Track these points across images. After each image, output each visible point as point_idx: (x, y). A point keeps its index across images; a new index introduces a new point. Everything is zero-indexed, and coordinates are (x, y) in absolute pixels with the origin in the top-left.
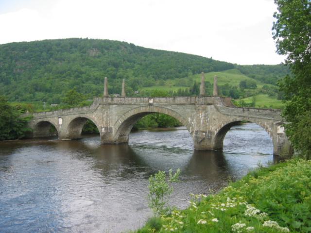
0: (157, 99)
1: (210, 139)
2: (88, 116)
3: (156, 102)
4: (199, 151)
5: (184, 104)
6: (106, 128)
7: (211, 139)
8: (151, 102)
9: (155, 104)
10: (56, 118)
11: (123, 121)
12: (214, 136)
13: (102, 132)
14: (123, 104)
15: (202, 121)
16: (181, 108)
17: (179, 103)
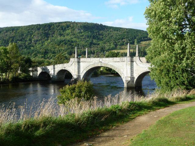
2: (67, 69)
5: (119, 62)
7: (134, 81)
8: (101, 60)
12: (135, 80)
14: (86, 62)
16: (117, 63)
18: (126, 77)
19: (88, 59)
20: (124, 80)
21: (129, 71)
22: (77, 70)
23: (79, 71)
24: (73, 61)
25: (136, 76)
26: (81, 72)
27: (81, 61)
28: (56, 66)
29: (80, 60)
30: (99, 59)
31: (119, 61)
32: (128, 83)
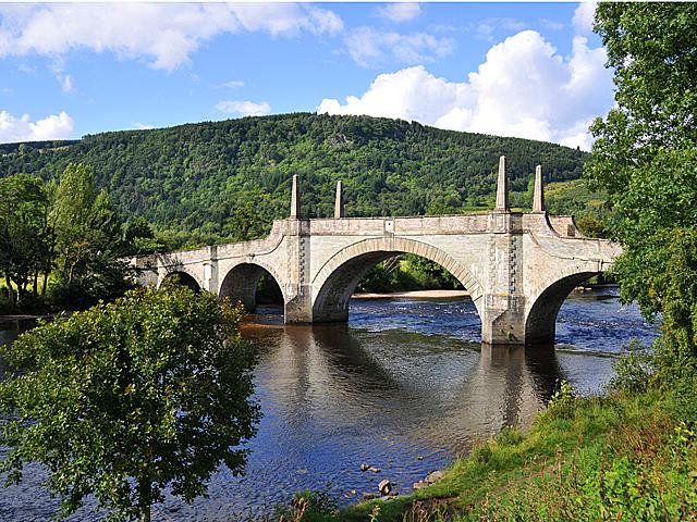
7: (522, 314)
8: (389, 228)
12: (528, 309)
14: (331, 234)
15: (499, 271)
19: (345, 222)
20: (481, 308)
21: (503, 270)
22: (295, 267)
24: (282, 231)
25: (531, 294)
26: (312, 277)
28: (221, 251)
29: (309, 226)
30: (379, 222)
31: (463, 229)
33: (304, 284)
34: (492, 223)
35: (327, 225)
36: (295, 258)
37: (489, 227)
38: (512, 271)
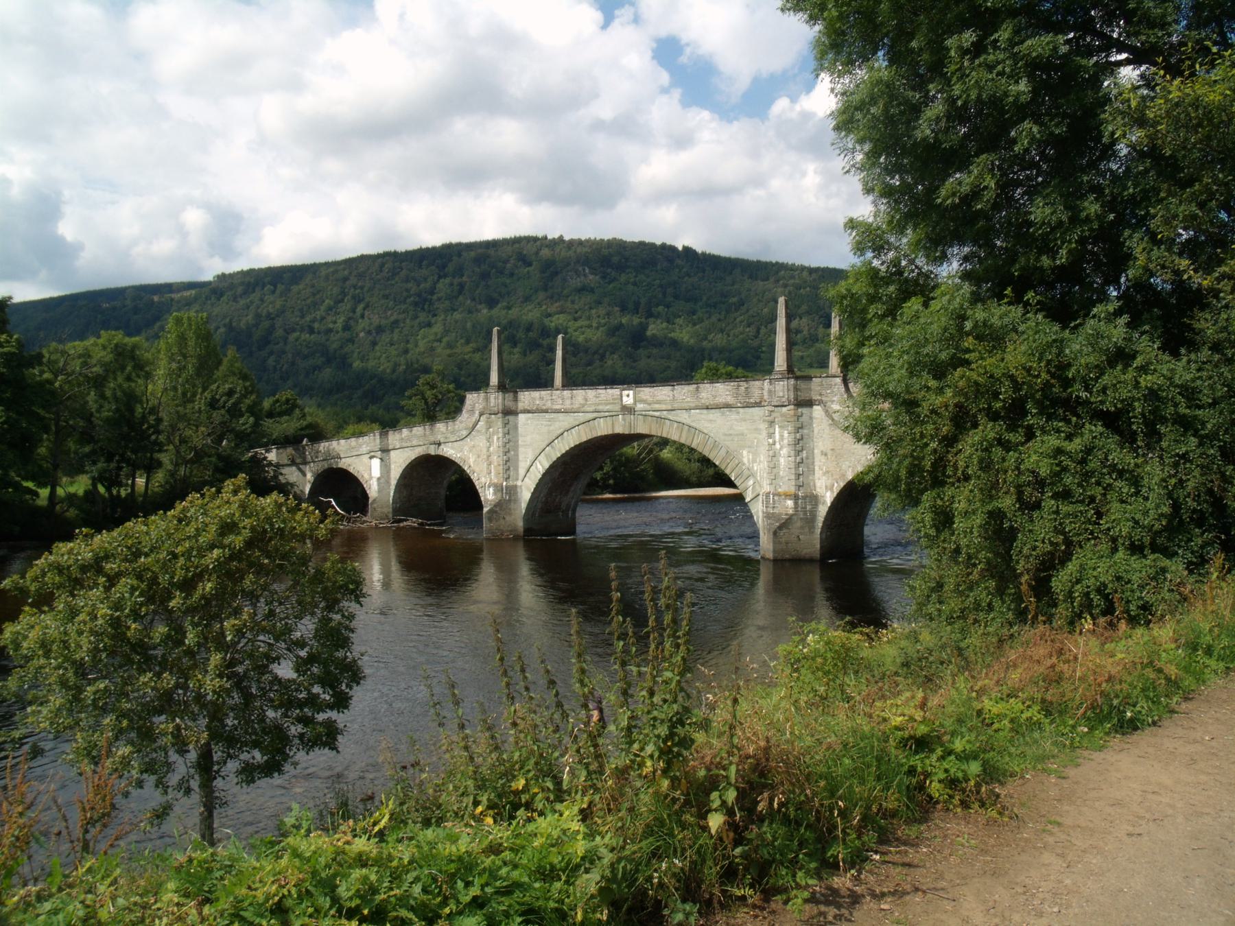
0: (646, 392)
1: (811, 520)
2: (449, 451)
3: (642, 401)
4: (783, 561)
5: (728, 406)
6: (498, 488)
9: (640, 406)
10: (365, 458)
11: (547, 465)
12: (823, 511)
13: (487, 500)
14: (546, 411)
15: (782, 460)
17: (711, 402)
18: (768, 494)
19: (567, 393)
20: (758, 510)
23: (509, 464)
24: (479, 407)
25: (827, 491)
26: (521, 477)
27: (521, 406)
28: (394, 438)
29: (516, 399)
30: (614, 392)
31: (730, 400)
32: (780, 528)
33: (511, 483)
34: (770, 391)
35: (541, 398)
36: (497, 441)
37: (766, 397)
38: (798, 459)
